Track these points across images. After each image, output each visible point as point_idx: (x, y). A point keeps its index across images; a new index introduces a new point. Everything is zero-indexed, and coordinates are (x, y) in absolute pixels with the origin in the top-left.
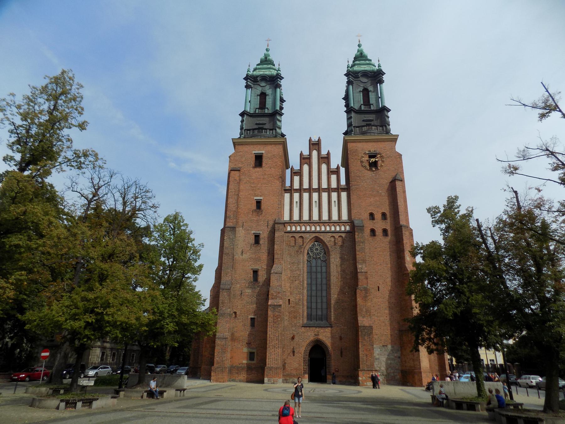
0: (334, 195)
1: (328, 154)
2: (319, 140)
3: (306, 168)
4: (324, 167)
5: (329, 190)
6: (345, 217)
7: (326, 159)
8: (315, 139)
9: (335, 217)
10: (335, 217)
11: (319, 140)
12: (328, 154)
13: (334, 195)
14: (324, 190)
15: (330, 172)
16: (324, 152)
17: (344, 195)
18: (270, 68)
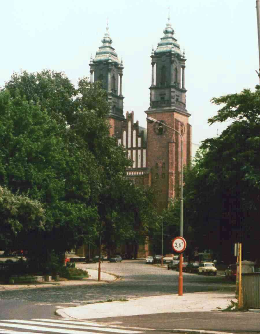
0: (139, 151)
1: (138, 122)
2: (133, 112)
3: (125, 133)
4: (134, 132)
5: (137, 148)
6: (144, 166)
7: (136, 126)
8: (130, 112)
9: (139, 166)
10: (139, 166)
11: (133, 112)
12: (138, 122)
13: (139, 151)
14: (134, 149)
15: (138, 136)
16: (135, 122)
17: (144, 151)
18: (105, 53)
